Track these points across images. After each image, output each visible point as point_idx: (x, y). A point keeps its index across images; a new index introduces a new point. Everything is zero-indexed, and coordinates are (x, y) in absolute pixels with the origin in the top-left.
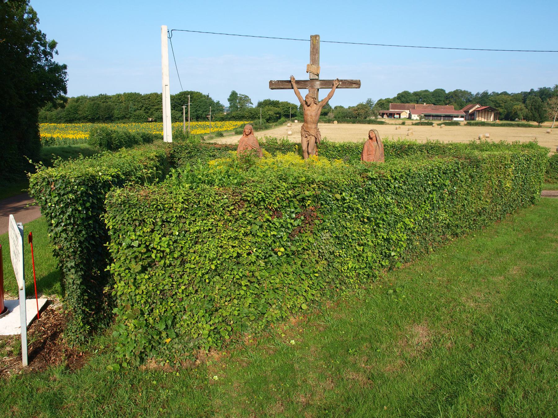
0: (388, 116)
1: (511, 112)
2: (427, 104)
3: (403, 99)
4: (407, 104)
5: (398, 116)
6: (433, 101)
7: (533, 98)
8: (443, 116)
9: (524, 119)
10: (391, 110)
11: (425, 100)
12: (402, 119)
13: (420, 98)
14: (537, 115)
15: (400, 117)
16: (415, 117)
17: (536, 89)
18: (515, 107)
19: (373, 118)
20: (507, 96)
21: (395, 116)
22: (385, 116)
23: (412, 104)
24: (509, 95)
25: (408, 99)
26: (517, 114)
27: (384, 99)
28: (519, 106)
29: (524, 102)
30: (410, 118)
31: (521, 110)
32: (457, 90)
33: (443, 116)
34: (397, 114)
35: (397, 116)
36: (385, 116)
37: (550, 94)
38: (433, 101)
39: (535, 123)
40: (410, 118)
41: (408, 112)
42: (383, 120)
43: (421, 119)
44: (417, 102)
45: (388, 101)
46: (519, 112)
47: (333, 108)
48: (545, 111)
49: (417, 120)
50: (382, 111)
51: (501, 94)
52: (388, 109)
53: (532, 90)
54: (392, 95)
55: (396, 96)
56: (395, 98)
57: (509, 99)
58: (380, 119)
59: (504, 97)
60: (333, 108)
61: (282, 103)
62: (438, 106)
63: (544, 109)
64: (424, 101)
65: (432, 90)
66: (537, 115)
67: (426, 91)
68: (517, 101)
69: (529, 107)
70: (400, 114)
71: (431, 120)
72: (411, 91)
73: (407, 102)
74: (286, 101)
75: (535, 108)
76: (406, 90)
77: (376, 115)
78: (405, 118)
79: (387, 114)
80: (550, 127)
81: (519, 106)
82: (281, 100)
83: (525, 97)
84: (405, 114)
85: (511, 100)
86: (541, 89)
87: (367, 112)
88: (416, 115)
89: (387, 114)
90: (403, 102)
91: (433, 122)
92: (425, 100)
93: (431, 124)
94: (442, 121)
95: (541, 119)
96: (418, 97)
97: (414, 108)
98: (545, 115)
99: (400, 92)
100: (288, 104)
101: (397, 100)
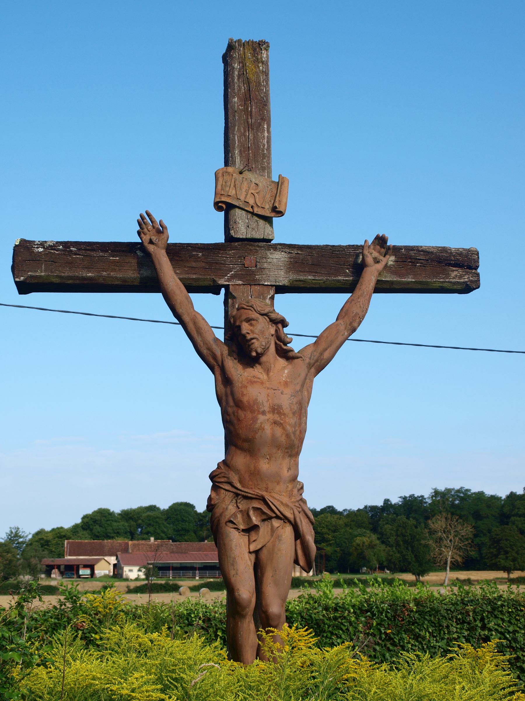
0: (62, 573)
1: (350, 554)
2: (156, 539)
3: (97, 529)
4: (107, 542)
5: (88, 572)
6: (170, 532)
7: (394, 520)
8: (200, 569)
9: (382, 568)
11: (150, 529)
12: (101, 579)
13: (139, 526)
14: (410, 557)
15: (93, 574)
16: (133, 573)
17: (395, 500)
18: (358, 540)
19: (27, 578)
20: (336, 517)
21: (81, 572)
22: (55, 574)
23: (120, 541)
24: (340, 513)
25: (109, 530)
26: (364, 558)
27: (48, 528)
28: (365, 539)
29: (374, 530)
30: (118, 573)
31: (371, 546)
33: (200, 569)
34: (85, 566)
35: (84, 572)
36: (55, 574)
37: (425, 510)
38: (170, 532)
39: (410, 577)
40: (118, 573)
41: (113, 560)
42: (53, 583)
43: (147, 575)
44: (132, 536)
45: (59, 534)
46: (369, 553)
48: (427, 546)
49: (137, 579)
50: (49, 561)
51: (323, 511)
52: (61, 555)
53: (387, 501)
54: (69, 519)
55: (79, 521)
56: (76, 526)
57: (341, 522)
58: (44, 581)
59: (330, 518)
62: (184, 545)
63: (423, 542)
64: (148, 533)
65: (164, 505)
66: (410, 557)
67: (152, 508)
68: (359, 526)
69: (392, 540)
70: (92, 568)
71: (170, 578)
72: (117, 508)
73: (108, 537)
75: (405, 542)
76: (104, 506)
77: (34, 571)
78: (106, 576)
79: (58, 567)
80: (442, 585)
81: (365, 539)
83: (374, 518)
84: (104, 567)
85: (346, 525)
86: (405, 498)
87: (11, 561)
88: (135, 569)
89: (58, 567)
90: (97, 537)
91: (180, 583)
92: (150, 529)
93: (175, 588)
94: (197, 581)
95: (421, 565)
96: (133, 523)
97: (125, 550)
98: (428, 557)
99: (90, 511)
101: (81, 533)
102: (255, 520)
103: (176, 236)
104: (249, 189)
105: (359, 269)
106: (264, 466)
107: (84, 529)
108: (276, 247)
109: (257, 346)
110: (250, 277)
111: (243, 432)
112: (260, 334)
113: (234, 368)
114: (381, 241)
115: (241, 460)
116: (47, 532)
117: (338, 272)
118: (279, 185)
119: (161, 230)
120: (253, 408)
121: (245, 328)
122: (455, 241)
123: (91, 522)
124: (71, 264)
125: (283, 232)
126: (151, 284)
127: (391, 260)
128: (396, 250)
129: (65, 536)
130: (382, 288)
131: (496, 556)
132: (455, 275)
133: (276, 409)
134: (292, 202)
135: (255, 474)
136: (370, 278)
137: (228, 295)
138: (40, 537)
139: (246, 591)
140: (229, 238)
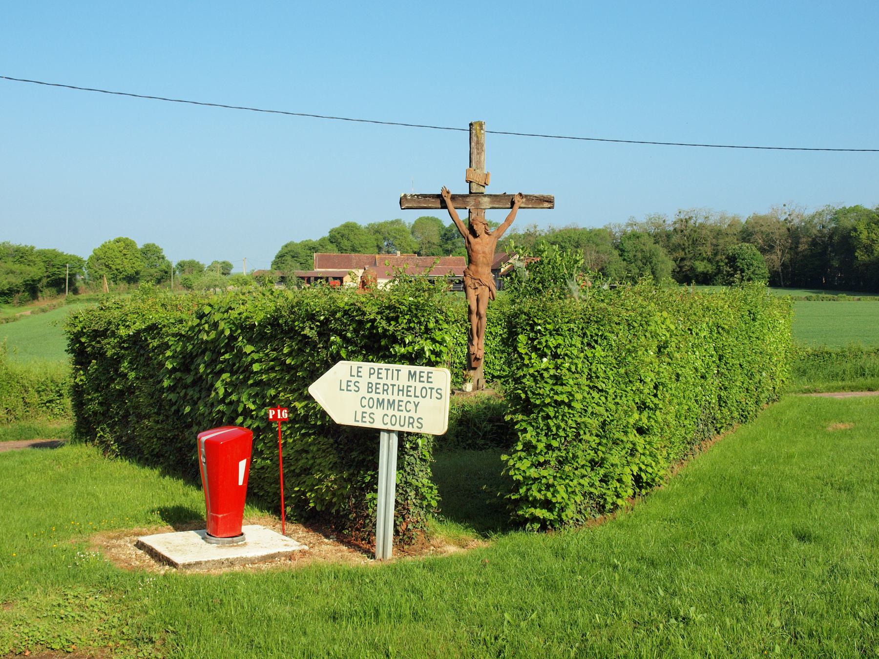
10: (319, 271)
13: (385, 239)
27: (297, 240)
32: (420, 218)
41: (360, 272)
47: (174, 265)
54: (318, 233)
55: (327, 235)
56: (323, 239)
60: (174, 265)
61: (42, 253)
74: (51, 248)
82: (40, 246)
97: (374, 264)
100: (57, 255)
101: (330, 246)
102: (477, 286)
103: (452, 192)
104: (477, 177)
105: (513, 203)
106: (480, 269)
107: (332, 242)
108: (485, 196)
109: (478, 233)
110: (478, 206)
111: (474, 259)
112: (480, 229)
113: (471, 237)
114: (520, 194)
115: (473, 267)
116: (297, 245)
117: (507, 203)
118: (487, 175)
119: (448, 193)
120: (477, 253)
121: (475, 227)
122: (545, 193)
123: (338, 236)
124: (419, 202)
125: (487, 191)
126: (444, 206)
127: (524, 200)
128: (526, 196)
129: (314, 248)
130: (520, 208)
131: (732, 275)
132: (546, 205)
133: (484, 253)
134: (491, 181)
135: (477, 272)
136: (516, 206)
137: (470, 212)
138: (289, 249)
139: (474, 308)
140: (470, 193)
